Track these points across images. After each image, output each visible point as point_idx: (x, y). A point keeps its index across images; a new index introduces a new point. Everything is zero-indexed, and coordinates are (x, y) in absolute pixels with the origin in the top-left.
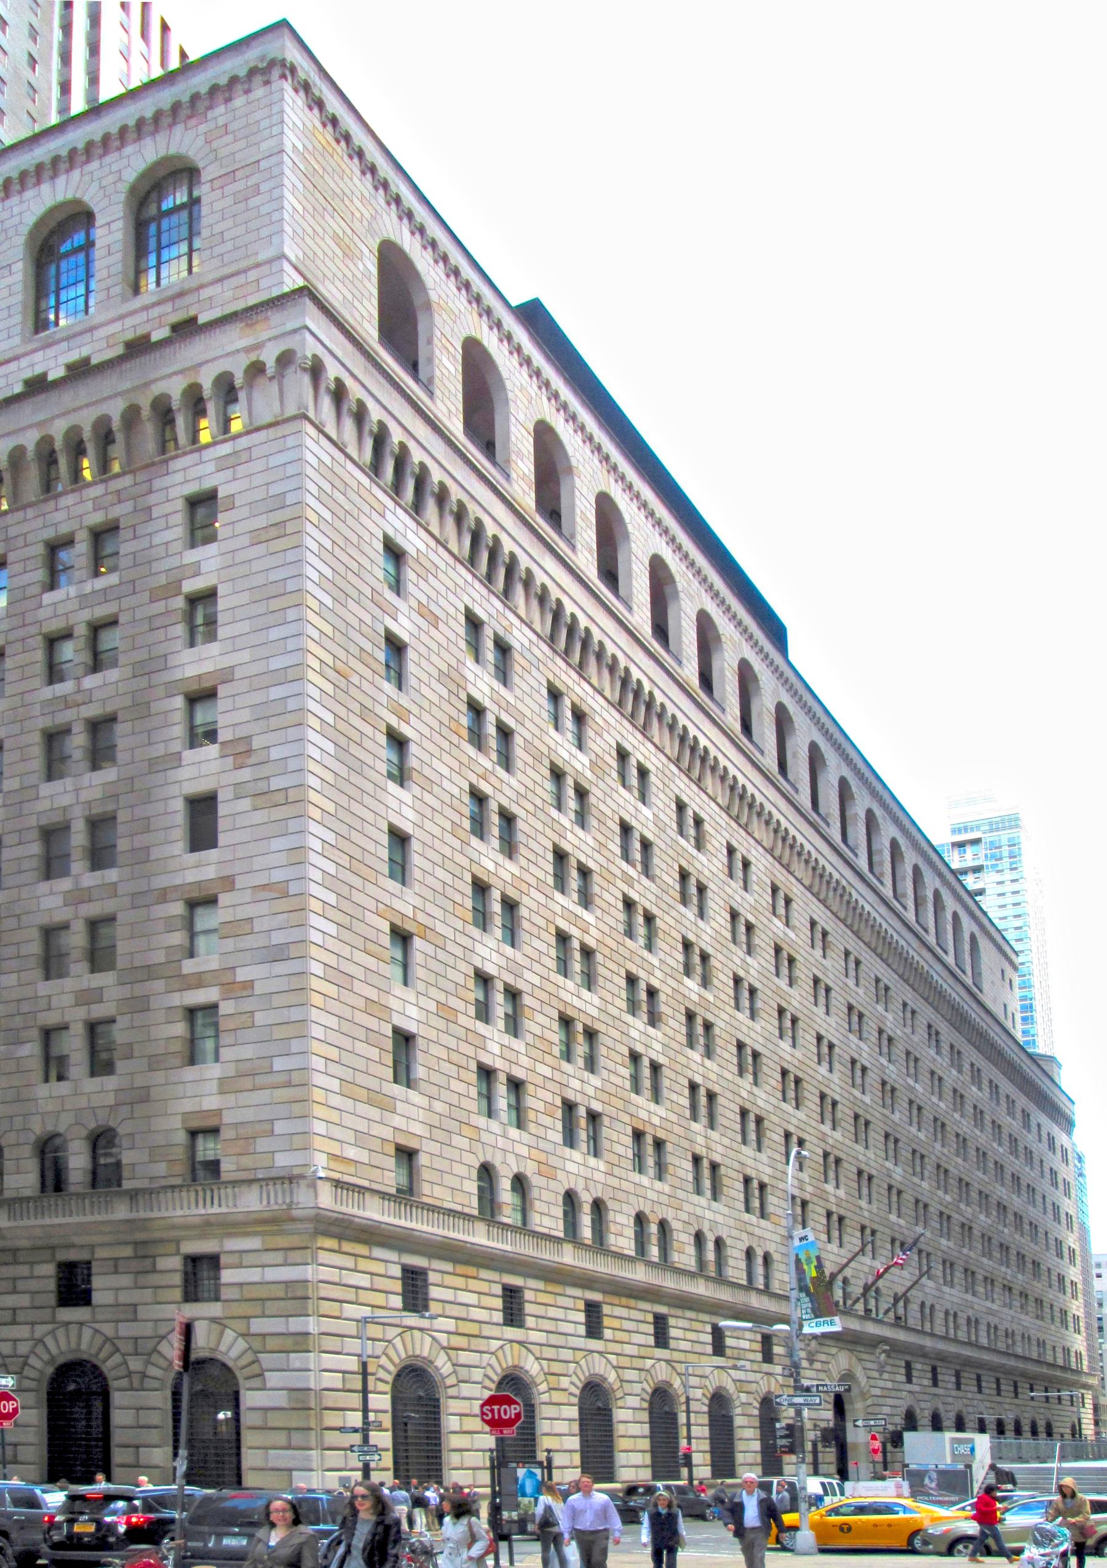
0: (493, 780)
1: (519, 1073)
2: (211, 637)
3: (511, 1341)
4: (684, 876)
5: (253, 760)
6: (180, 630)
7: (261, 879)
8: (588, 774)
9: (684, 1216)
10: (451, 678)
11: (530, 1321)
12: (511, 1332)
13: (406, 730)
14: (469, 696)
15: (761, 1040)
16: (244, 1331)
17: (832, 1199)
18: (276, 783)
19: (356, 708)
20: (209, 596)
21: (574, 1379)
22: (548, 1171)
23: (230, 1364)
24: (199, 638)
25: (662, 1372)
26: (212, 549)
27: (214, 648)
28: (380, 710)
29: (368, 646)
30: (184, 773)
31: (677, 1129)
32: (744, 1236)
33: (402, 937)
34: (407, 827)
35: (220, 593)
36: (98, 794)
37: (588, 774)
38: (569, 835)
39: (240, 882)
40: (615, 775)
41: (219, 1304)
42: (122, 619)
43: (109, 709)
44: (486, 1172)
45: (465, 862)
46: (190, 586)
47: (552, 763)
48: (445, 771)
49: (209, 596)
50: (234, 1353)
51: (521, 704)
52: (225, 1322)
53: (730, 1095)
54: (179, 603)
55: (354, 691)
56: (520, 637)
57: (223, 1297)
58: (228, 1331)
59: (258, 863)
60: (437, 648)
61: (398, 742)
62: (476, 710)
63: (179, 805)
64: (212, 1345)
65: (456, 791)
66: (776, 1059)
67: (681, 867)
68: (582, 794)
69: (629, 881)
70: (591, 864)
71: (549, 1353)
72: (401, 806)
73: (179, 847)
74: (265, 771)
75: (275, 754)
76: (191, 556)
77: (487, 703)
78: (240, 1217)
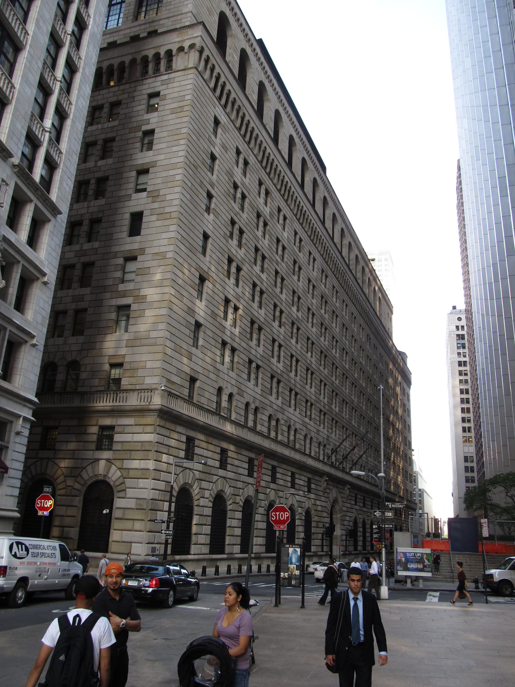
0: (239, 216)
1: (236, 345)
2: (150, 148)
3: (221, 477)
4: (295, 262)
5: (159, 199)
6: (138, 145)
7: (156, 250)
8: (268, 217)
9: (285, 418)
10: (230, 174)
11: (229, 467)
12: (221, 472)
13: (213, 192)
14: (234, 181)
15: (315, 337)
16: (121, 467)
17: (334, 413)
18: (167, 210)
19: (199, 181)
20: (152, 132)
21: (242, 497)
22: (241, 392)
23: (112, 484)
24: (145, 148)
25: (272, 496)
26: (155, 114)
27: (150, 153)
28: (205, 183)
29: (205, 158)
30: (131, 203)
31: (285, 376)
32: (304, 429)
33: (202, 279)
34: (209, 233)
35: (156, 132)
36: (96, 209)
37: (268, 217)
38: (260, 242)
39: (147, 251)
40: (276, 219)
41: (111, 452)
42: (117, 139)
43: (106, 174)
44: (220, 390)
45: (226, 250)
46: (145, 128)
47: (258, 211)
48: (224, 211)
49: (152, 132)
50: (114, 479)
51: (249, 183)
52: (112, 461)
53: (304, 362)
54: (140, 134)
55: (198, 174)
56: (252, 160)
57: (113, 449)
58: (113, 466)
59: (156, 243)
60: (225, 160)
61: (210, 196)
62: (236, 187)
63: (127, 216)
64: (105, 474)
65: (226, 219)
66: (319, 346)
67: (294, 259)
68: (265, 224)
69: (277, 263)
70: (266, 255)
71: (233, 483)
72: (209, 222)
73: (125, 234)
74: (163, 204)
75: (168, 197)
76: (146, 116)
77: (239, 184)
78: (127, 408)
